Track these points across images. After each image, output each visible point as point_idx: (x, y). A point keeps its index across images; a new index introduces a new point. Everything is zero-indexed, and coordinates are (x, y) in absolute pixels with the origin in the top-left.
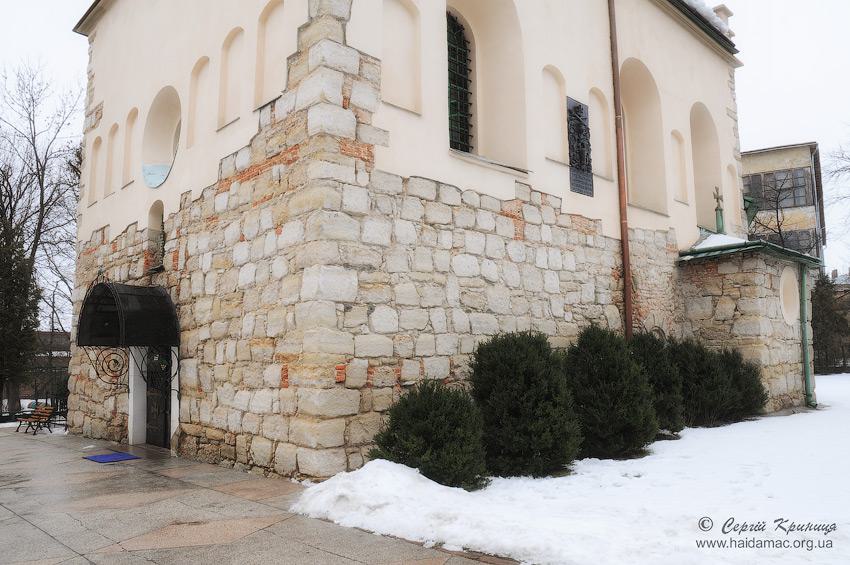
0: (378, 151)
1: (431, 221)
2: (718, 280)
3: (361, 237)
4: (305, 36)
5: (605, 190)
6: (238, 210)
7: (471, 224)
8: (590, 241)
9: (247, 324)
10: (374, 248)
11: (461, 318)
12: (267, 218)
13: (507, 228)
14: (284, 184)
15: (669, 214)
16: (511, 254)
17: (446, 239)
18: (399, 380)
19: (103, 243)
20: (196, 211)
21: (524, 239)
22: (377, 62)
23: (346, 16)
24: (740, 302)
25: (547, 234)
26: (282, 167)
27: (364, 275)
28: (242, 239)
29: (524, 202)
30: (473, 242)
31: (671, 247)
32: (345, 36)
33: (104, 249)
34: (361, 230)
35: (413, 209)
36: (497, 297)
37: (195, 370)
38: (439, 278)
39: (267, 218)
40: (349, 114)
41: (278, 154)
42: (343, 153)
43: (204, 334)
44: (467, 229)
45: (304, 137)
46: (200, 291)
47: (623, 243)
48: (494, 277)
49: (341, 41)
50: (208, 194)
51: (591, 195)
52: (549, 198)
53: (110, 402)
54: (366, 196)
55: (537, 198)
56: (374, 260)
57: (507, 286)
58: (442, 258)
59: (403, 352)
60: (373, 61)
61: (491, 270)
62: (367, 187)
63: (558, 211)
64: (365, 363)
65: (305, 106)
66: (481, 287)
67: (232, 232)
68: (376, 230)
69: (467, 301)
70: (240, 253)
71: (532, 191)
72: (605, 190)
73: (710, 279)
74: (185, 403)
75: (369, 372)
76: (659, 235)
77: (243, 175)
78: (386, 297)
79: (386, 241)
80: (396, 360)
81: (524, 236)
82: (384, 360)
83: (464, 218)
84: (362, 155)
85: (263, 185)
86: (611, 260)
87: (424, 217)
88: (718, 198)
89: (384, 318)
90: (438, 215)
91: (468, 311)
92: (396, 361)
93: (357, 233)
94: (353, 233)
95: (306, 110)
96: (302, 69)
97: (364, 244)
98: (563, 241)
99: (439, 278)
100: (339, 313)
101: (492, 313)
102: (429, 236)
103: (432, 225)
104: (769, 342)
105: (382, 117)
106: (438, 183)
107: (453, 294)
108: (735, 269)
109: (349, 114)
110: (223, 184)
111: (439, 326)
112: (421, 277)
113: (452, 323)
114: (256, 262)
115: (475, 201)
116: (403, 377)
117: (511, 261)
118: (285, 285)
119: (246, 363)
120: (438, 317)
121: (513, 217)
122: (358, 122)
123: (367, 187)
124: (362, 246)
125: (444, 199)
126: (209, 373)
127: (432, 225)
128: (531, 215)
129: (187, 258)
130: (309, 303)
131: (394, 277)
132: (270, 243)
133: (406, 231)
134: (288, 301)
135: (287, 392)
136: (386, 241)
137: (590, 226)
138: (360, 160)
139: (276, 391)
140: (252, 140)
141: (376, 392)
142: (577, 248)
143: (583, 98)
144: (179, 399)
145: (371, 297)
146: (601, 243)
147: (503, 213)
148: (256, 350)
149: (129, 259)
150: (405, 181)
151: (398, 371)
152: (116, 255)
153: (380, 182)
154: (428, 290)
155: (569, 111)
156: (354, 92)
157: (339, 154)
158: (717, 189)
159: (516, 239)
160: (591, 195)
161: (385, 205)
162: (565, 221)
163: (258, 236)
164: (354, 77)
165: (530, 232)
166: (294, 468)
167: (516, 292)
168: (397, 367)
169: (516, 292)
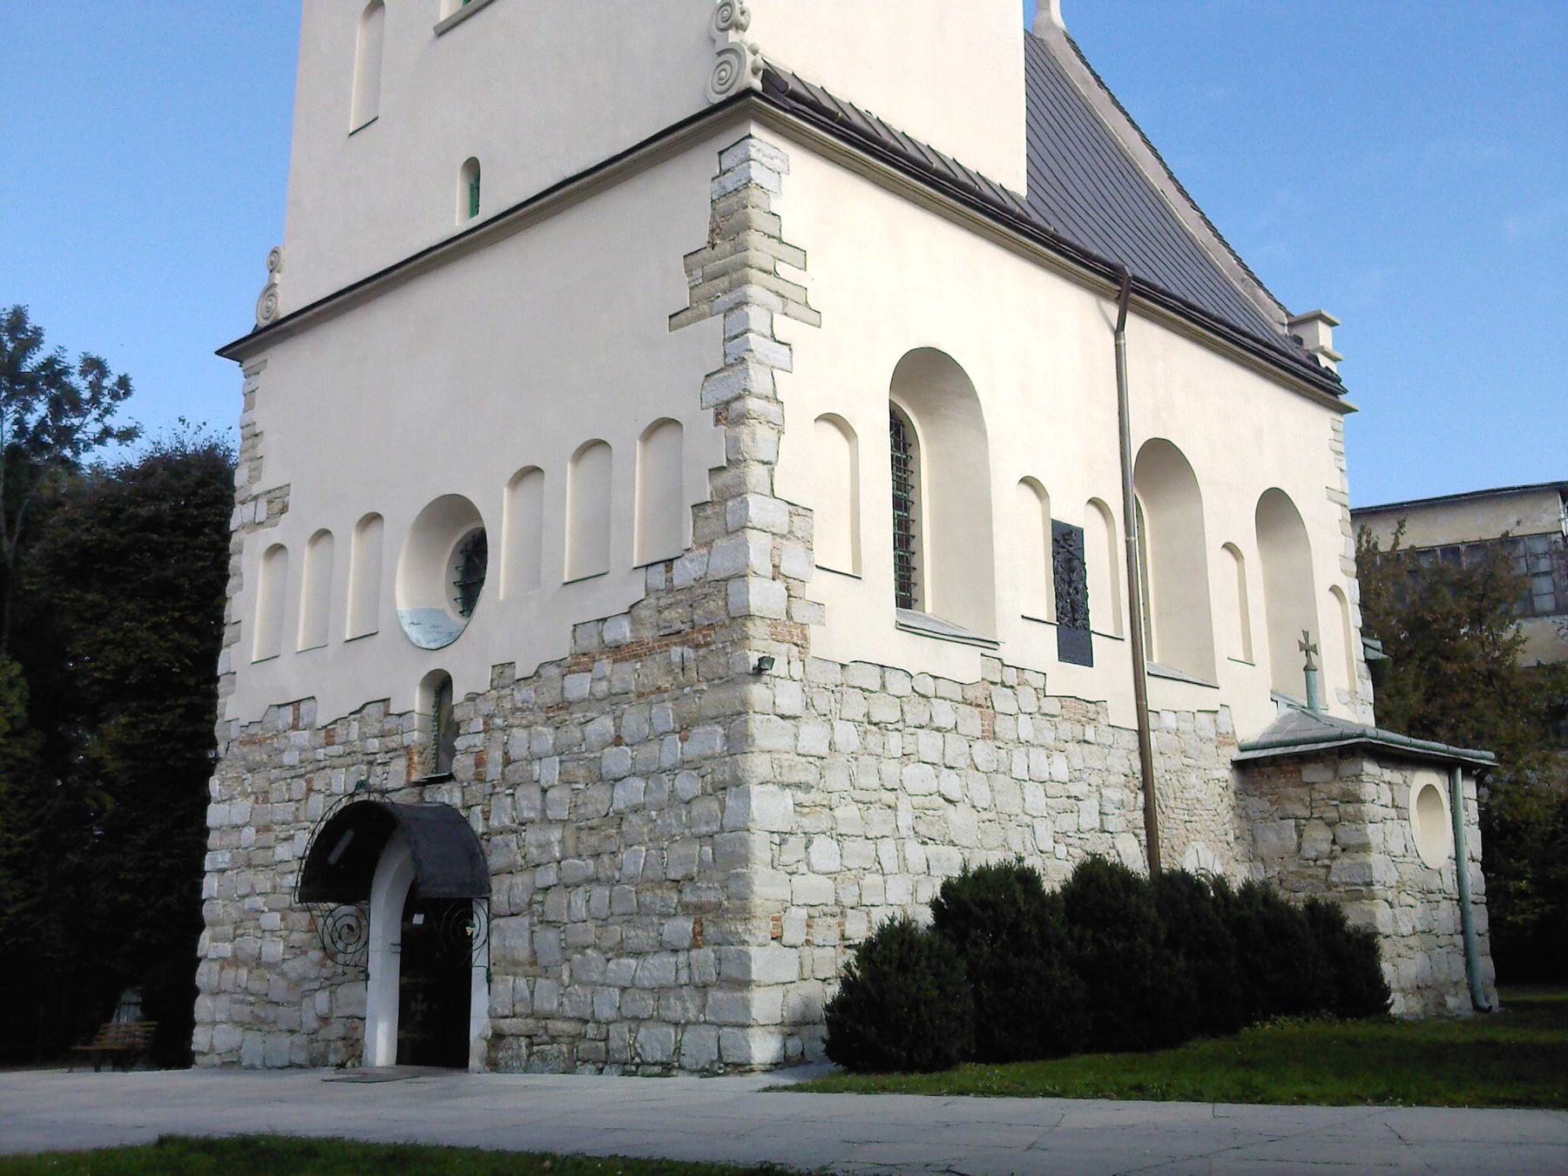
0: (813, 632)
1: (875, 720)
2: (1303, 792)
3: (796, 746)
5: (1111, 656)
6: (613, 700)
7: (924, 720)
8: (1090, 736)
9: (635, 859)
10: (811, 759)
11: (915, 853)
12: (665, 715)
13: (972, 722)
15: (1220, 683)
16: (978, 760)
17: (895, 742)
18: (843, 938)
19: (295, 727)
20: (524, 694)
21: (994, 736)
22: (808, 513)
23: (773, 460)
24: (1339, 830)
25: (1026, 728)
26: (689, 653)
27: (801, 796)
28: (618, 741)
29: (992, 683)
30: (928, 745)
31: (1224, 739)
32: (772, 484)
33: (302, 737)
34: (796, 737)
35: (855, 706)
36: (959, 817)
37: (527, 934)
38: (888, 797)
39: (665, 715)
40: (779, 586)
41: (679, 632)
42: (773, 640)
43: (548, 876)
44: (922, 727)
45: (722, 615)
46: (532, 815)
47: (1142, 733)
48: (954, 794)
49: (768, 492)
50: (546, 672)
51: (1089, 662)
52: (1027, 675)
53: (322, 1000)
54: (800, 693)
55: (1011, 677)
56: (810, 777)
57: (974, 807)
58: (891, 769)
59: (849, 899)
60: (804, 512)
61: (951, 784)
62: (801, 680)
63: (1041, 692)
64: (804, 912)
65: (723, 575)
66: (939, 808)
67: (604, 725)
68: (813, 737)
69: (922, 829)
71: (1003, 665)
72: (1111, 656)
73: (1291, 791)
74: (503, 985)
75: (809, 926)
76: (1204, 719)
77: (618, 652)
78: (825, 824)
79: (824, 751)
80: (837, 910)
81: (994, 733)
82: (825, 909)
83: (917, 713)
84: (795, 640)
85: (652, 672)
86: (1125, 760)
87: (868, 715)
88: (1309, 649)
89: (824, 853)
90: (885, 711)
91: (924, 843)
92: (841, 911)
93: (792, 742)
94: (784, 742)
95: (726, 580)
96: (715, 525)
97: (799, 755)
98: (1049, 737)
99: (888, 797)
100: (774, 847)
101: (955, 845)
102: (873, 741)
103: (876, 724)
104: (1390, 895)
105: (819, 587)
106: (882, 666)
107: (905, 819)
108: (1329, 775)
109: (779, 586)
110: (580, 662)
111: (889, 864)
112: (866, 797)
113: (904, 859)
114: (646, 775)
115: (927, 686)
116: (847, 934)
117: (978, 770)
118: (698, 809)
119: (625, 918)
120: (887, 850)
121: (979, 706)
122: (789, 596)
123: (801, 680)
124: (798, 758)
125: (891, 689)
126: (551, 935)
127: (876, 724)
128: (1004, 701)
129: (507, 762)
131: (835, 797)
132: (672, 750)
133: (846, 735)
134: (704, 829)
135: (708, 953)
136: (824, 751)
137: (1088, 710)
138: (793, 647)
139: (682, 957)
140: (632, 607)
141: (817, 952)
142: (1071, 746)
143: (1074, 513)
144: (489, 980)
145: (808, 823)
146: (1107, 737)
147: (965, 702)
148: (647, 898)
149: (371, 758)
150: (843, 666)
151: (840, 925)
152: (336, 750)
153: (817, 674)
154: (875, 813)
155: (1055, 540)
156: (784, 557)
157: (771, 641)
158: (1306, 634)
159: (984, 738)
160: (1089, 662)
161: (823, 701)
162: (1051, 706)
164: (783, 536)
165: (1003, 727)
166: (715, 1057)
167: (985, 815)
168: (838, 919)
169: (985, 815)
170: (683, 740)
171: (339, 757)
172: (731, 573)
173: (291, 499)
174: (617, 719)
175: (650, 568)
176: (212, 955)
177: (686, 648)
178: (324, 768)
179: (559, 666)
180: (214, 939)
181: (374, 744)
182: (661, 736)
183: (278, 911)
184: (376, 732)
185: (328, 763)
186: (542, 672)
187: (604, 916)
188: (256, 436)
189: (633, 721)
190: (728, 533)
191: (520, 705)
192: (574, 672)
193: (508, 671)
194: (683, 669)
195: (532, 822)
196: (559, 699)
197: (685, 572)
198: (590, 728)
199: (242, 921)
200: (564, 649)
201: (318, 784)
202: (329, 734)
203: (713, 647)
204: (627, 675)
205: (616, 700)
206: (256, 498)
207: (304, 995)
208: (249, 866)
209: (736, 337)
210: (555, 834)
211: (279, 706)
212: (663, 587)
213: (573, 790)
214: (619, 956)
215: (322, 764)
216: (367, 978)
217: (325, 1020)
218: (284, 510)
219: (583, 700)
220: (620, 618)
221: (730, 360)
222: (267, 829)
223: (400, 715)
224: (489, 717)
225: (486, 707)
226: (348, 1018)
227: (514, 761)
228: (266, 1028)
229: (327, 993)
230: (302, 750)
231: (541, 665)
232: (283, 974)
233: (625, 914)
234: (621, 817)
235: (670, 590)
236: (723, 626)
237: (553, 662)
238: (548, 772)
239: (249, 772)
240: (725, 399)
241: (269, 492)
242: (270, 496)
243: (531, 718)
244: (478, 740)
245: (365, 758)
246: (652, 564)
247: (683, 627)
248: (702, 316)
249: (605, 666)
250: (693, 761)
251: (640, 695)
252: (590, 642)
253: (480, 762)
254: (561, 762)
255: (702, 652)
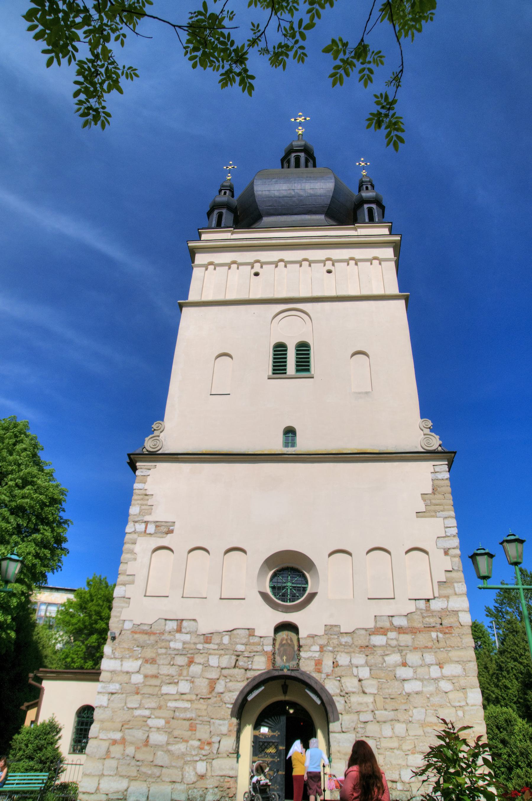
4: (449, 574)
9: (418, 714)
12: (429, 658)
14: (442, 644)
20: (344, 639)
26: (440, 635)
43: (367, 717)
46: (354, 690)
65: (456, 609)
70: (403, 672)
77: (400, 630)
85: (422, 639)
96: (449, 591)
114: (421, 680)
118: (451, 696)
119: (417, 737)
130: (474, 708)
132: (435, 672)
134: (458, 704)
149: (240, 653)
163: (421, 666)
170: (441, 667)
171: (215, 650)
172: (461, 609)
173: (176, 528)
174: (404, 657)
175: (417, 601)
176: (102, 736)
177: (439, 633)
178: (201, 654)
179: (366, 630)
180: (102, 729)
181: (240, 648)
182: (429, 665)
183: (163, 718)
184: (244, 642)
185: (205, 651)
186: (357, 631)
187: (403, 735)
188: (146, 495)
189: (413, 658)
190: (456, 594)
191: (344, 643)
192: (378, 634)
193: (336, 629)
194: (438, 641)
195: (353, 693)
196: (367, 644)
197: (436, 605)
198: (386, 658)
199: (129, 721)
200: (371, 625)
201: (199, 659)
202: (207, 638)
203: (453, 635)
204: (406, 639)
205: (401, 648)
206: (147, 523)
207: (186, 763)
208: (137, 693)
209: (450, 527)
210: (369, 699)
211: (166, 620)
212: (424, 608)
213: (379, 682)
214: (413, 753)
215: (201, 651)
216: (238, 757)
217: (202, 777)
218: (171, 532)
219: (383, 646)
220: (402, 617)
221: (448, 534)
222: (156, 677)
223: (261, 637)
224: (322, 647)
225: (323, 641)
226: (222, 776)
227: (341, 666)
228: (150, 780)
229: (205, 762)
230: (184, 643)
231: (357, 629)
232: (168, 751)
233: (415, 736)
234: (409, 695)
235: (428, 609)
236: (458, 627)
237: (363, 629)
238: (364, 673)
239: (138, 646)
240: (449, 547)
241: (157, 522)
242: (157, 524)
243: (352, 650)
244: (317, 655)
245: (235, 653)
246: (418, 599)
247: (436, 625)
248: (432, 516)
249: (392, 635)
250: (448, 677)
251: (415, 648)
252: (387, 625)
253: (318, 663)
254: (370, 670)
255: (447, 636)
